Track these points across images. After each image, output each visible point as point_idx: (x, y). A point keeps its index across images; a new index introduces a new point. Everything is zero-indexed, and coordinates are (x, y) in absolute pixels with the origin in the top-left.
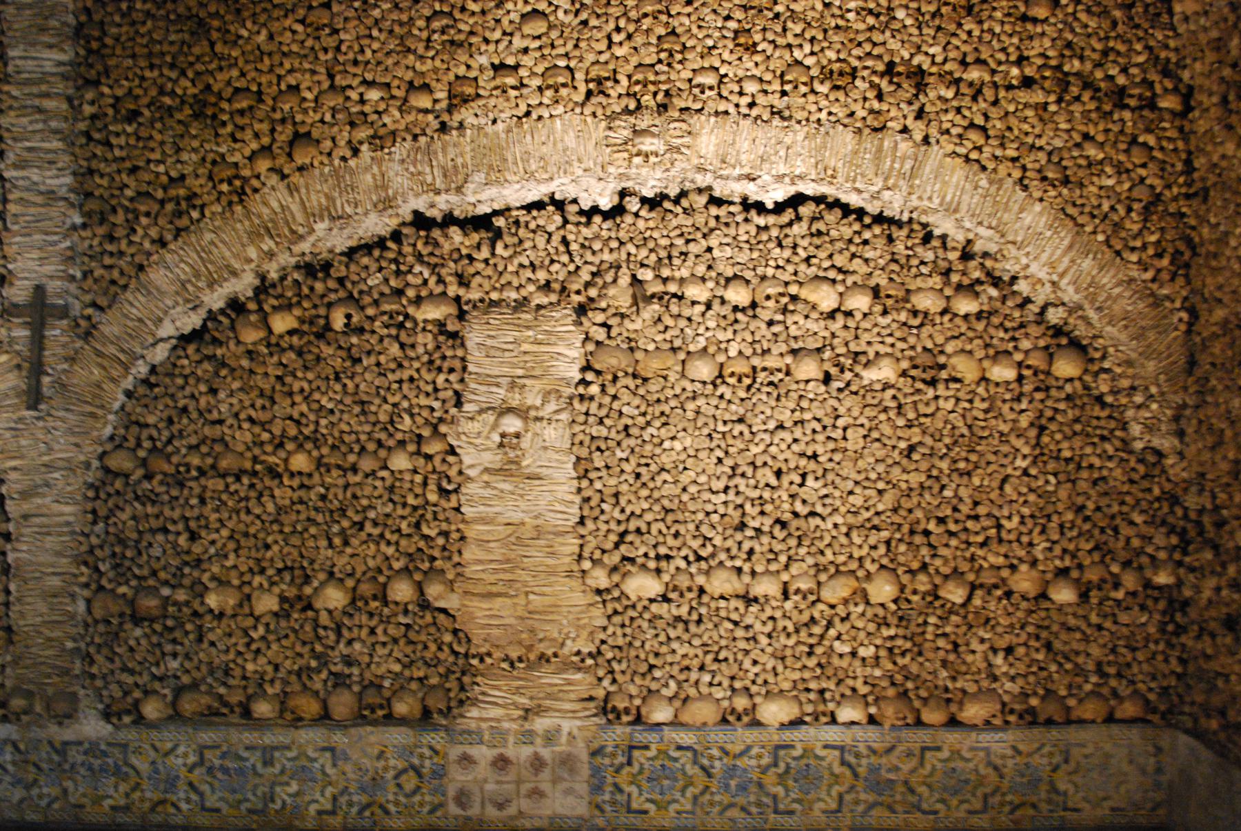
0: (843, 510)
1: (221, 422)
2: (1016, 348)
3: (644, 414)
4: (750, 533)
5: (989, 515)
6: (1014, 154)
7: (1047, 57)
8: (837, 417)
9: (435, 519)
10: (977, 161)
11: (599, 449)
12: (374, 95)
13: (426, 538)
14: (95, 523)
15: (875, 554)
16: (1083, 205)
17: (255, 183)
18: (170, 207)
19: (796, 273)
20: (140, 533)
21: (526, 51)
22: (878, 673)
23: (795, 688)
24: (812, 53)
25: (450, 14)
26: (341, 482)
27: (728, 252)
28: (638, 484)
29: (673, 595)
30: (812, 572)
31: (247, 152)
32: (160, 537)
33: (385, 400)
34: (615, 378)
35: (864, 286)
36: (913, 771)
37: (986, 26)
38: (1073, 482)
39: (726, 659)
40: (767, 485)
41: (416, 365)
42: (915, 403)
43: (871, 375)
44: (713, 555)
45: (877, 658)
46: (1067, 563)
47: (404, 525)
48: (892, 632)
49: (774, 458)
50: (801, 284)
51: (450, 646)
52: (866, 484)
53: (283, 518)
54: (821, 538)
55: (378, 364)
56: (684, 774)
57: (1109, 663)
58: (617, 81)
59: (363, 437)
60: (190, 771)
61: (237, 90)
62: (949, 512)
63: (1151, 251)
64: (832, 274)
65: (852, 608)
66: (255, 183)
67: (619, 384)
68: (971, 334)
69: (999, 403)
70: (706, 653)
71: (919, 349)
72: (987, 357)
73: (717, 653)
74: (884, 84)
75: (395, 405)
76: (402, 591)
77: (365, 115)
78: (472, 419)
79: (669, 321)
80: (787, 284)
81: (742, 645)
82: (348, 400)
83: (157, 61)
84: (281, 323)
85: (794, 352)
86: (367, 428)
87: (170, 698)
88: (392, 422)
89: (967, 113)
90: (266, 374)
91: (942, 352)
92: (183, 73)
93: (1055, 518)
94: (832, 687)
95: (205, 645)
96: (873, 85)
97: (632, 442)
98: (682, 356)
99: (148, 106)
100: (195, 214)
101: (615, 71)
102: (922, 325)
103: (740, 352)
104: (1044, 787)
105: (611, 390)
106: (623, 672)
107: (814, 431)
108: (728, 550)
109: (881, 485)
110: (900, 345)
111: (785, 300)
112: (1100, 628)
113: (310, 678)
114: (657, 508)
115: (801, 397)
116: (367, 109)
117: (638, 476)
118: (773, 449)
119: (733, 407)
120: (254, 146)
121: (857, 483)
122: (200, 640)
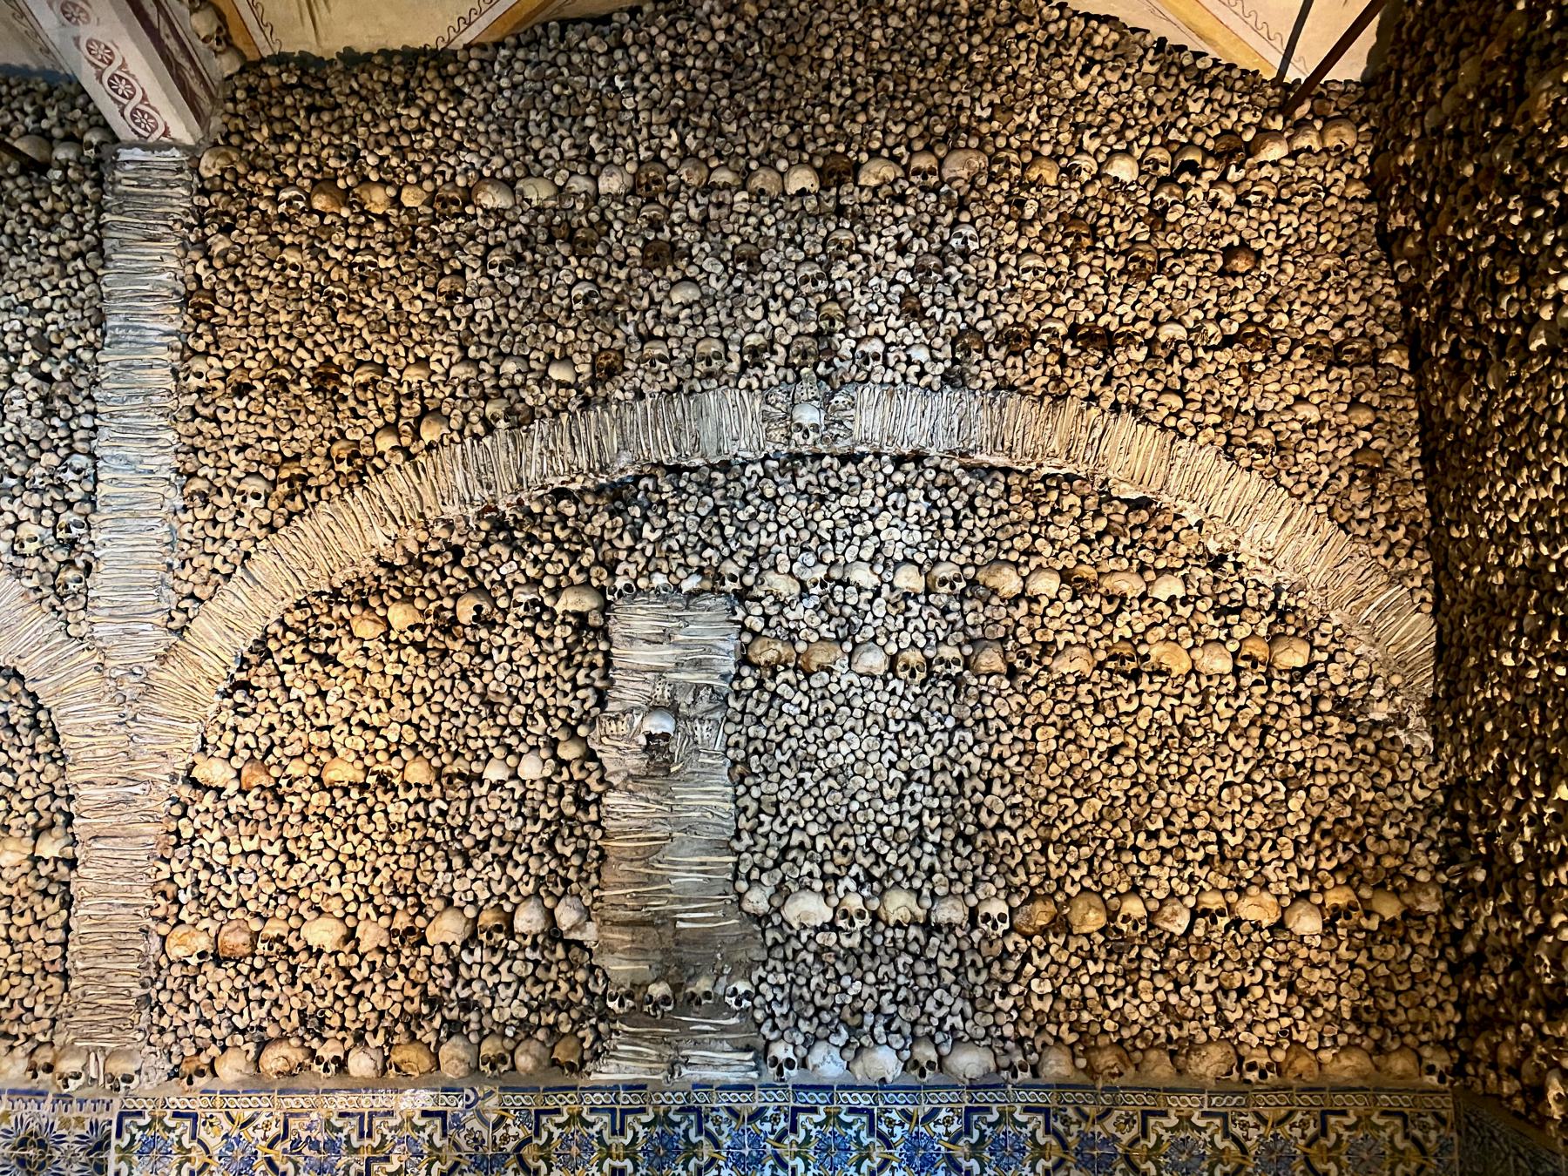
0: (1035, 823)
1: (329, 728)
2: (1229, 636)
3: (807, 713)
4: (928, 848)
5: (1208, 828)
6: (1218, 419)
7: (1251, 315)
8: (1025, 716)
9: (571, 835)
10: (1175, 428)
11: (756, 751)
12: (509, 367)
13: (561, 857)
14: (178, 845)
15: (1076, 875)
17: (377, 461)
18: (283, 488)
19: (973, 555)
20: (230, 856)
21: (676, 320)
22: (1086, 1017)
23: (987, 1034)
24: (986, 317)
25: (594, 281)
26: (463, 794)
27: (896, 534)
28: (800, 792)
29: (842, 923)
30: (1002, 895)
31: (371, 431)
32: (253, 859)
33: (516, 700)
34: (775, 674)
36: (1135, 1141)
37: (1179, 282)
38: (1307, 790)
39: (905, 1001)
41: (553, 660)
42: (1114, 699)
43: (1062, 666)
44: (889, 874)
45: (1084, 999)
46: (1305, 886)
47: (535, 844)
48: (1100, 968)
49: (953, 761)
50: (977, 567)
51: (585, 985)
53: (397, 837)
54: (1012, 855)
55: (510, 660)
56: (859, 1143)
57: (1367, 1009)
58: (774, 353)
59: (491, 743)
60: (271, 1146)
61: (360, 363)
62: (1160, 824)
63: (1382, 523)
64: (1014, 556)
65: (1051, 939)
66: (379, 463)
67: (779, 680)
68: (1173, 621)
70: (881, 993)
72: (1195, 646)
73: (895, 994)
74: (1067, 348)
75: (529, 707)
76: (528, 920)
77: (502, 390)
78: (616, 719)
79: (836, 610)
80: (962, 567)
81: (924, 982)
82: (475, 701)
83: (273, 332)
84: (400, 616)
85: (971, 641)
86: (497, 733)
87: (252, 1054)
88: (524, 725)
89: (1160, 376)
90: (383, 673)
92: (301, 344)
93: (1287, 831)
95: (299, 987)
96: (1053, 349)
97: (793, 743)
98: (848, 647)
99: (262, 380)
100: (311, 497)
101: (772, 341)
102: (1119, 611)
103: (913, 644)
105: (770, 685)
106: (785, 1016)
107: (998, 731)
108: (905, 868)
109: (1079, 794)
110: (1095, 634)
111: (960, 586)
112: (1352, 964)
113: (420, 1027)
114: (822, 818)
115: (982, 693)
116: (504, 383)
117: (801, 782)
118: (952, 752)
119: (905, 705)
120: (379, 422)
121: (1049, 791)
122: (293, 984)
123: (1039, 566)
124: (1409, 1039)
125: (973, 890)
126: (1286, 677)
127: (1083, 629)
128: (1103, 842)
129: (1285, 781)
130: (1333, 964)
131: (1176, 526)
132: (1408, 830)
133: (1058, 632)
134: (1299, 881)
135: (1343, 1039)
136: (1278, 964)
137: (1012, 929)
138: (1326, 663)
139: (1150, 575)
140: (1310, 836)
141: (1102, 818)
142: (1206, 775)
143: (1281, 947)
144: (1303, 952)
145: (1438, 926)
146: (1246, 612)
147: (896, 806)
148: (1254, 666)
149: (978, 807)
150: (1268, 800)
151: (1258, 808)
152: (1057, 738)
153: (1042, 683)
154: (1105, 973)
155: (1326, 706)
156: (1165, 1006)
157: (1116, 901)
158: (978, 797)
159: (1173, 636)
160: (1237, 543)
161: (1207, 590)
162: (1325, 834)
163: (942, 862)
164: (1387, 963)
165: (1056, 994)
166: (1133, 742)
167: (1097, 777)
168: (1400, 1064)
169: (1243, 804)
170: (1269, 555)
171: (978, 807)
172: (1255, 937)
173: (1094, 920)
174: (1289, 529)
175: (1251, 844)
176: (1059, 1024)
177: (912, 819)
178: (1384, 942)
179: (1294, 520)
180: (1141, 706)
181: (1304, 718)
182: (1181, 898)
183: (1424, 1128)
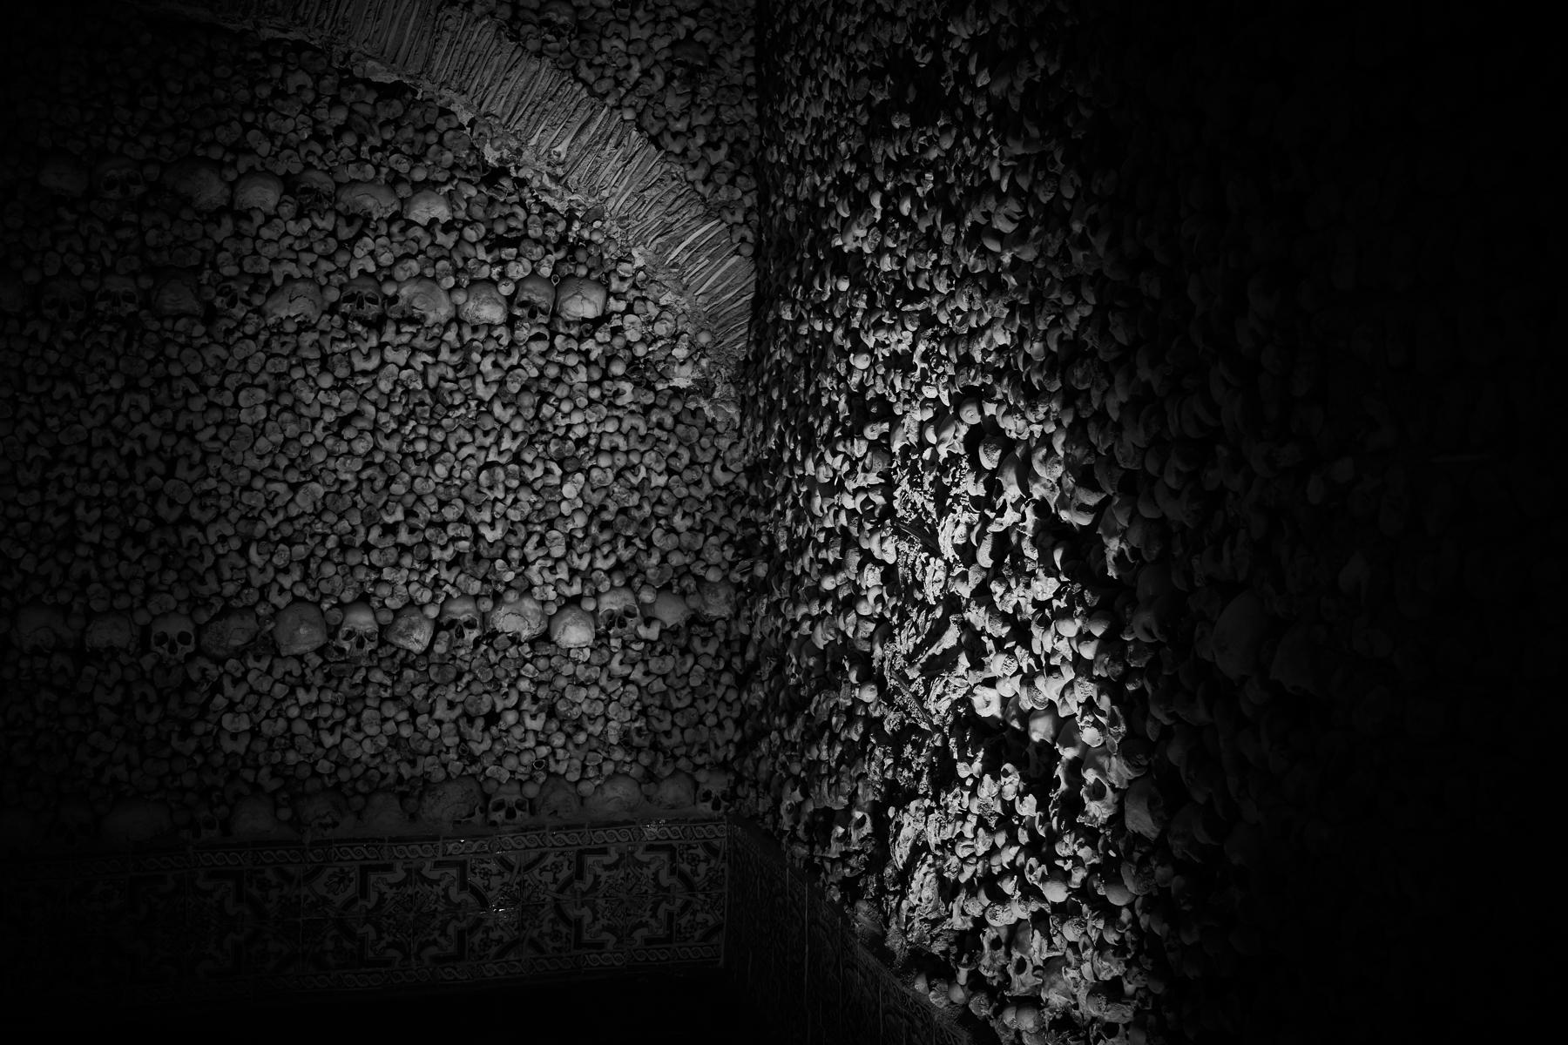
0: (234, 515)
2: (503, 275)
5: (463, 520)
15: (286, 582)
16: (603, 66)
22: (292, 757)
30: (183, 610)
35: (269, 174)
36: (353, 901)
40: (112, 476)
42: (348, 353)
46: (576, 589)
48: (313, 697)
49: (121, 435)
52: (272, 474)
54: (201, 558)
57: (639, 730)
62: (399, 516)
63: (700, 141)
64: (216, 153)
68: (432, 253)
69: (476, 357)
71: (354, 274)
72: (457, 286)
91: (390, 278)
93: (559, 524)
94: (222, 783)
102: (360, 235)
104: (548, 914)
107: (187, 394)
109: (293, 477)
110: (325, 266)
111: (138, 190)
112: (626, 680)
118: (119, 421)
119: (52, 356)
121: (255, 473)
123: (252, 170)
124: (682, 763)
125: (144, 604)
126: (574, 331)
127: (312, 258)
128: (325, 537)
129: (560, 464)
130: (603, 682)
131: (442, 125)
132: (704, 521)
133: (275, 261)
134: (569, 584)
135: (608, 768)
136: (538, 684)
137: (199, 651)
138: (623, 314)
139: (404, 191)
140: (586, 529)
141: (325, 509)
142: (465, 451)
143: (542, 663)
144: (568, 669)
145: (727, 633)
146: (526, 245)
147: (36, 495)
148: (532, 315)
149: (154, 495)
150: (538, 485)
151: (524, 495)
152: (268, 404)
153: (249, 329)
154: (319, 702)
155: (618, 369)
156: (395, 740)
157: (336, 613)
158: (155, 481)
159: (429, 272)
160: (519, 152)
161: (478, 212)
162: (604, 526)
163: (102, 570)
164: (664, 677)
165: (255, 732)
166: (371, 409)
167: (318, 456)
168: (671, 791)
169: (507, 490)
170: (560, 171)
171: (154, 495)
172: (512, 651)
173: (306, 638)
174: (585, 139)
175: (512, 540)
176: (258, 768)
177: (57, 513)
178: (664, 653)
179: (593, 128)
180: (383, 363)
181: (591, 384)
182: (422, 607)
183: (694, 860)
